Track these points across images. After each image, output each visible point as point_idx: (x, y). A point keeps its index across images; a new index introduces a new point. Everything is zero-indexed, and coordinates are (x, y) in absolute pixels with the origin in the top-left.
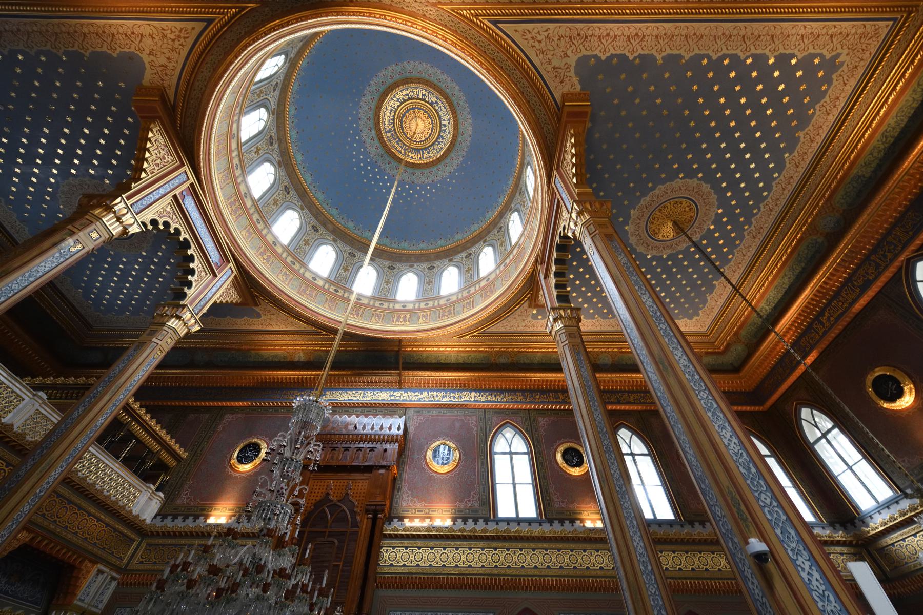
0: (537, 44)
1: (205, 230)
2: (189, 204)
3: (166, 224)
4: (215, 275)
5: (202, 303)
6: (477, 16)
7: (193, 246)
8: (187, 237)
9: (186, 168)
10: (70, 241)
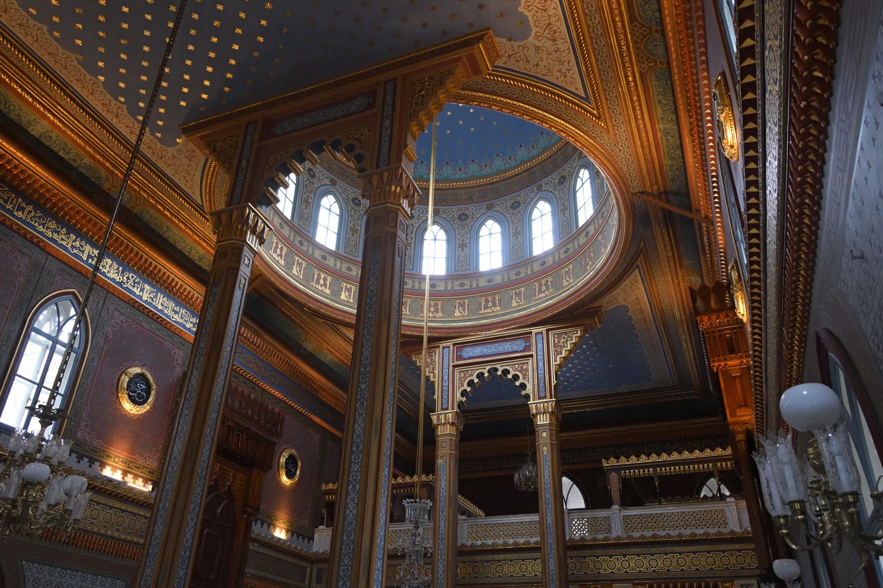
0: (188, 178)
1: (493, 346)
2: (468, 352)
3: (471, 383)
4: (531, 356)
5: (542, 385)
6: (208, 220)
7: (498, 366)
8: (488, 367)
9: (443, 344)
10: (440, 461)
